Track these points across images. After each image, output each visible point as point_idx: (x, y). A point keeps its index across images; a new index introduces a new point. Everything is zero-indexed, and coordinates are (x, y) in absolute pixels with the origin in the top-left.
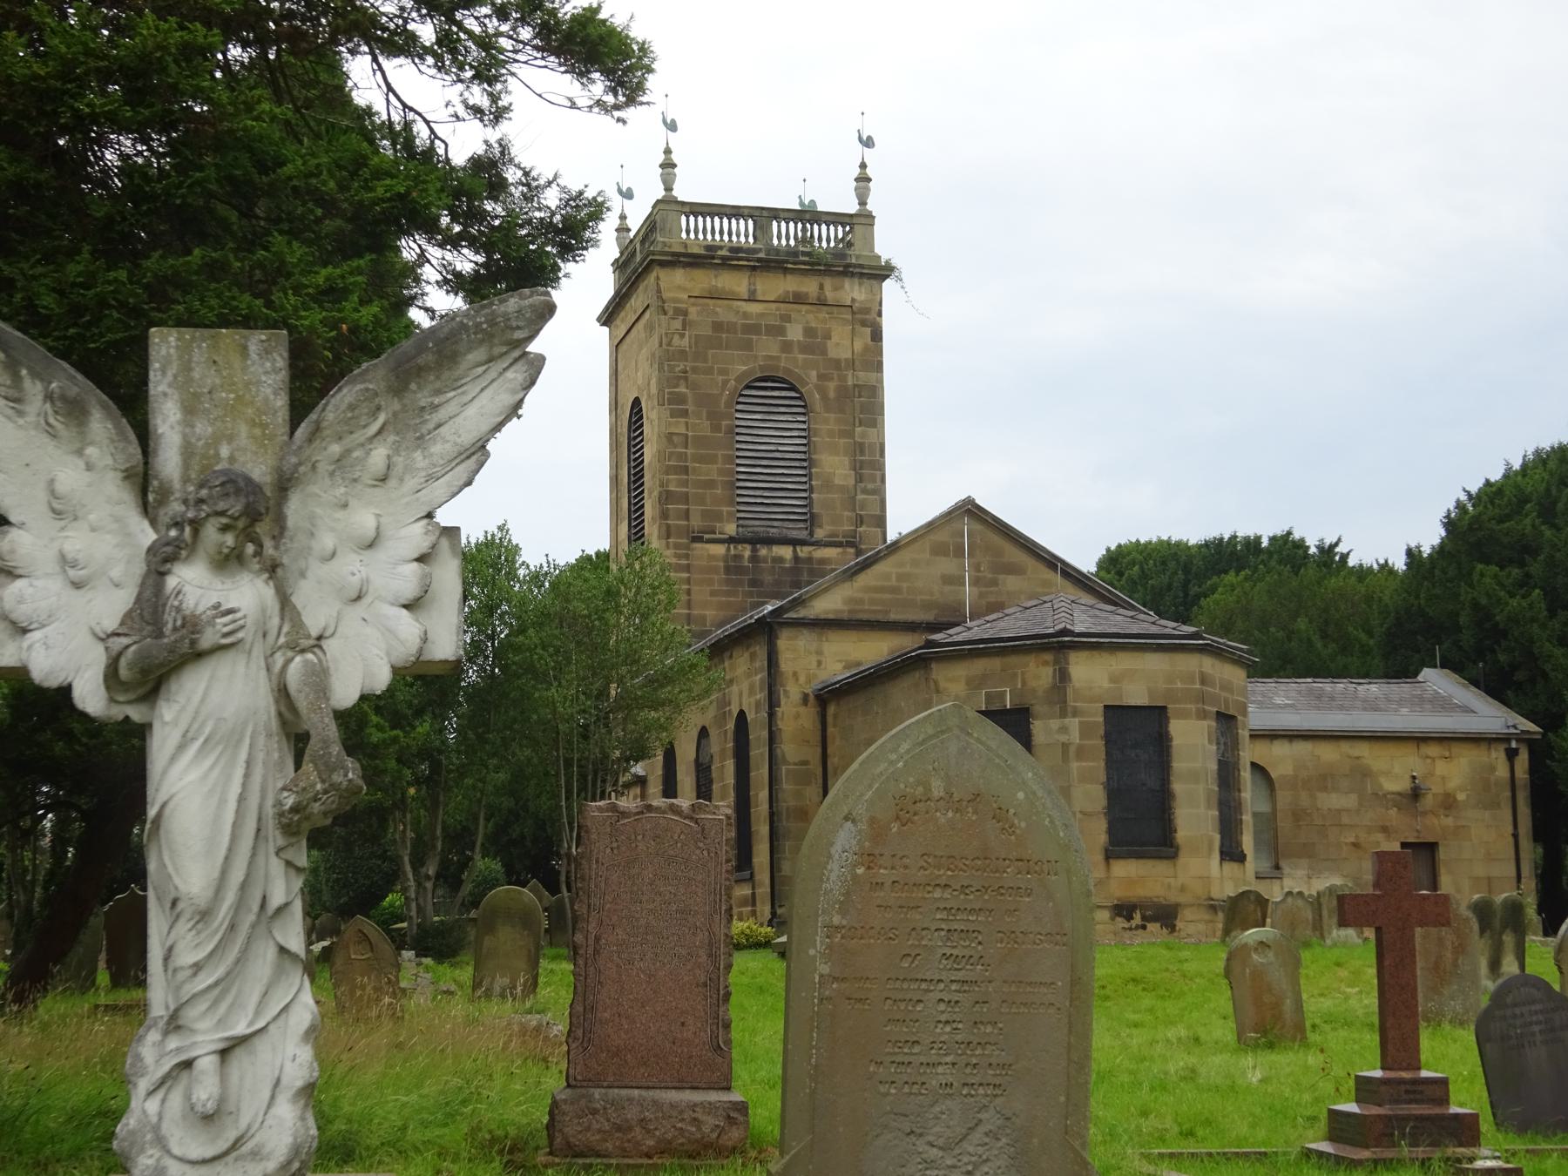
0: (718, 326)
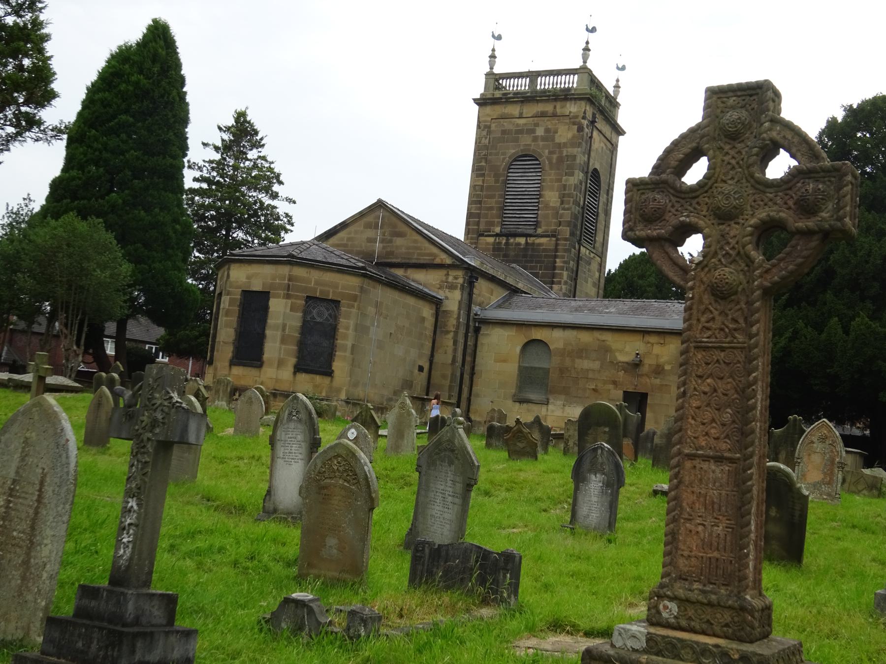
0: (504, 132)
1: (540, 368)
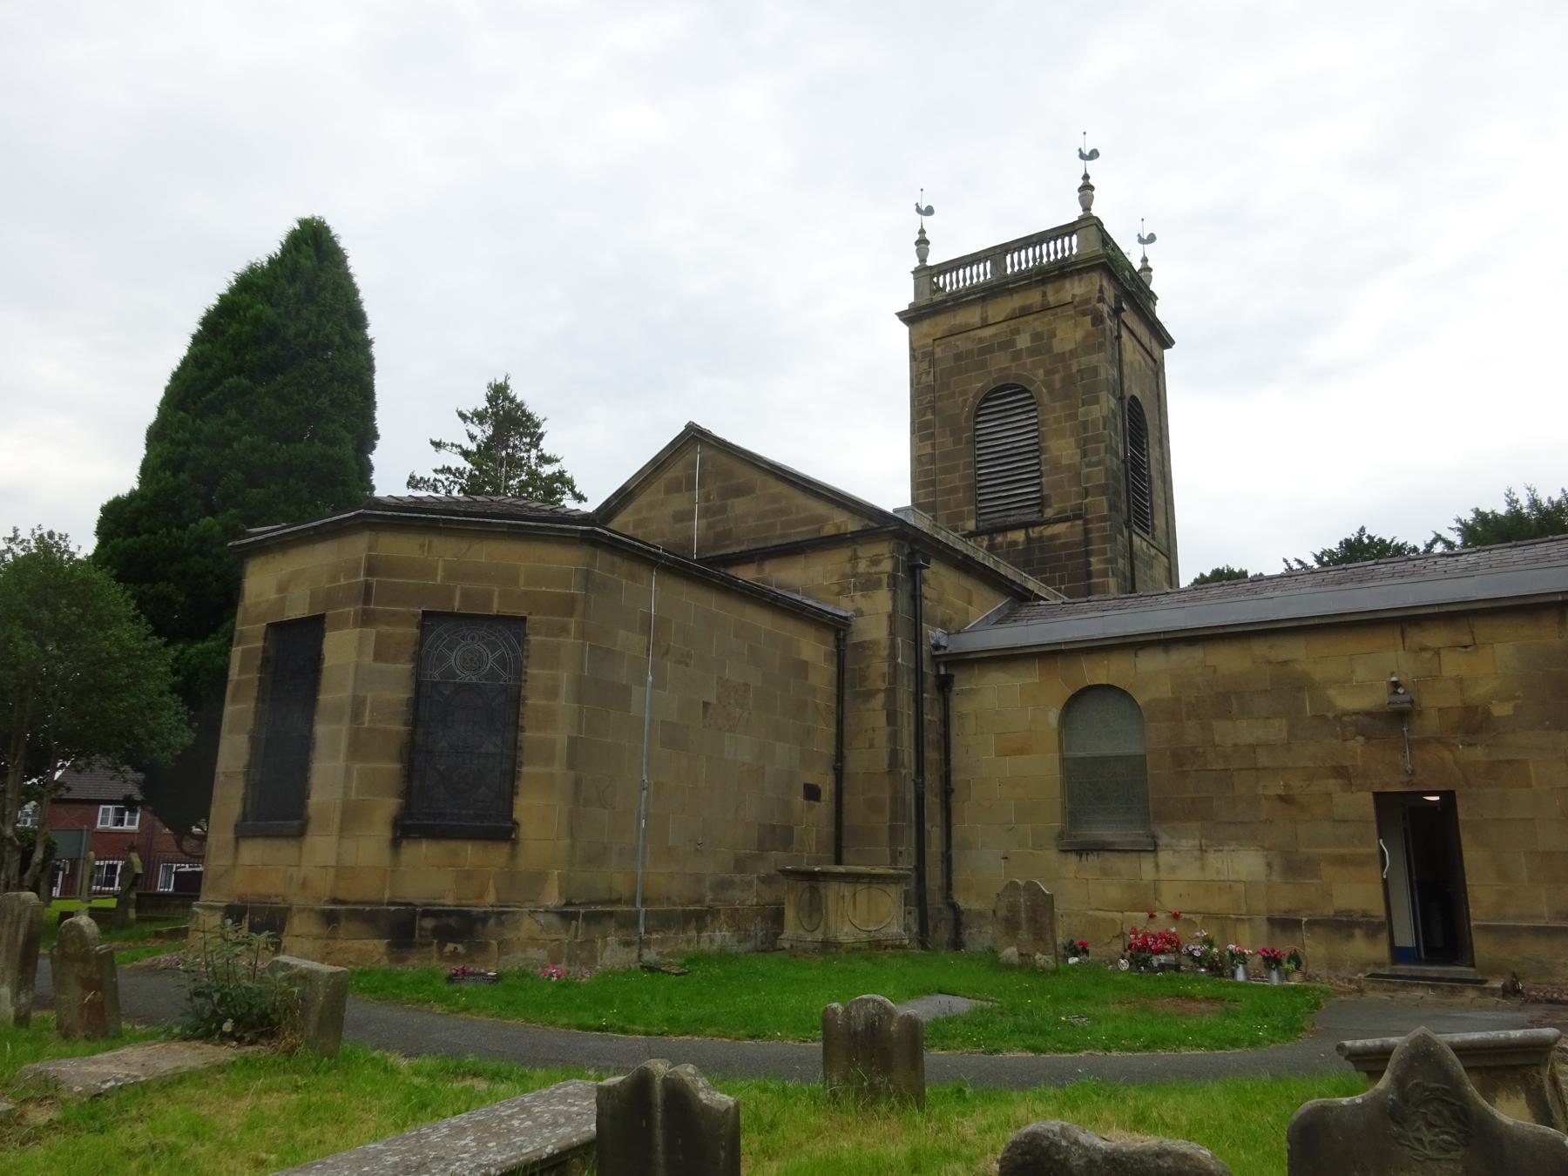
0: (958, 357)
1: (1117, 758)
